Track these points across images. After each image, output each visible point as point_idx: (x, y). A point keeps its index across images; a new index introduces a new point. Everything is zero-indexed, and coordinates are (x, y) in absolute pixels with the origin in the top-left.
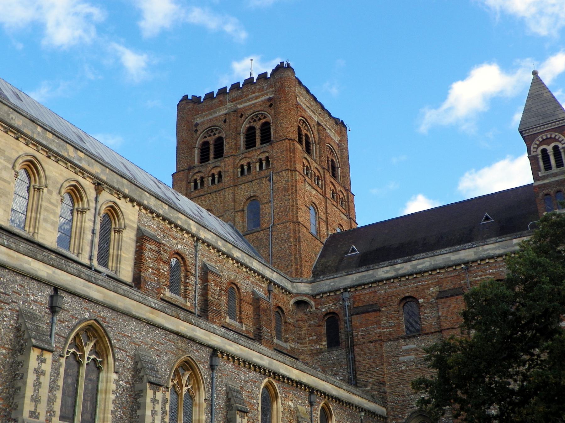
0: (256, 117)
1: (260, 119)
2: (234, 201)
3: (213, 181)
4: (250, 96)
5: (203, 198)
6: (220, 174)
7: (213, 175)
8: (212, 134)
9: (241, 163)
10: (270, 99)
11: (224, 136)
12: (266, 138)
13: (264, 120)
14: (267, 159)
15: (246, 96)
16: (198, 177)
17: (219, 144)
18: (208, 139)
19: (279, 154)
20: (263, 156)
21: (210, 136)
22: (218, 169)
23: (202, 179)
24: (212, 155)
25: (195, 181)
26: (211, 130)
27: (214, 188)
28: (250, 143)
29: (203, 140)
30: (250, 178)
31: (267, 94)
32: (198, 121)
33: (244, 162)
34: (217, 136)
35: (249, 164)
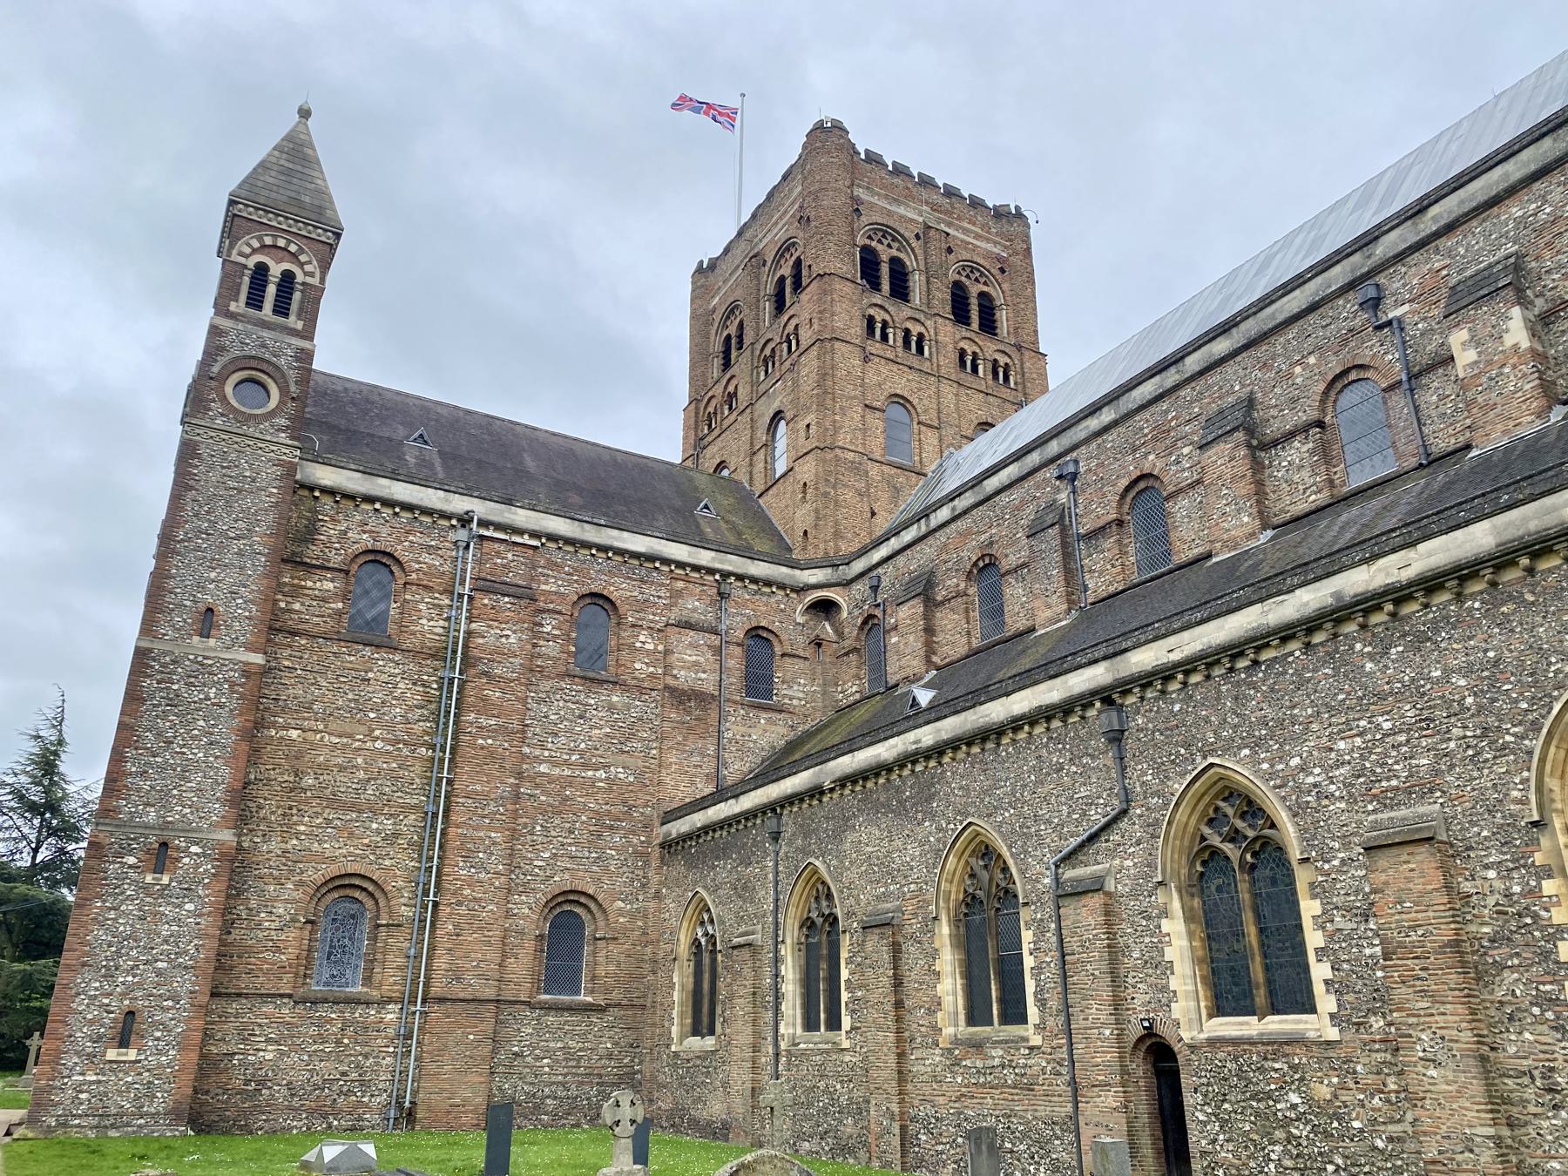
1: (977, 280)
4: (966, 225)
5: (895, 368)
6: (921, 337)
8: (886, 242)
13: (985, 289)
14: (1007, 368)
15: (959, 218)
19: (1035, 376)
21: (880, 241)
26: (885, 232)
27: (914, 361)
29: (868, 242)
31: (995, 243)
34: (894, 253)
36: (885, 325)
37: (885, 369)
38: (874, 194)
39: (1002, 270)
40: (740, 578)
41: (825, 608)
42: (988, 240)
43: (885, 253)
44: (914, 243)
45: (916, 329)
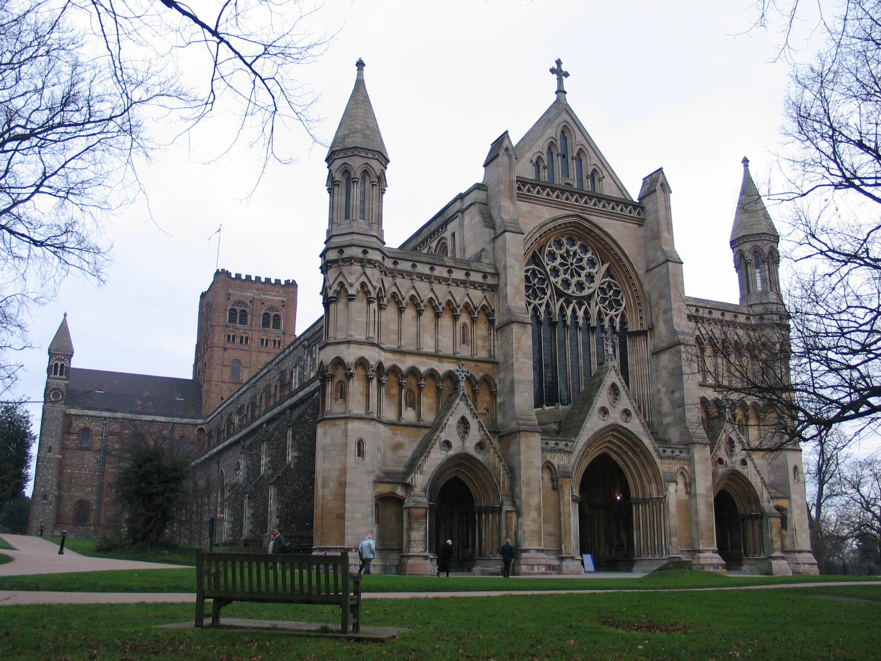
0: (272, 308)
2: (257, 361)
3: (241, 342)
4: (270, 293)
7: (242, 338)
9: (263, 337)
10: (283, 301)
11: (248, 311)
12: (277, 325)
13: (277, 313)
14: (279, 342)
16: (231, 334)
17: (244, 314)
18: (235, 307)
20: (277, 339)
22: (246, 335)
23: (234, 337)
24: (238, 321)
25: (229, 336)
26: (239, 303)
27: (243, 347)
28: (266, 324)
30: (267, 350)
31: (281, 296)
32: (230, 291)
33: (265, 338)
34: (242, 308)
35: (267, 340)
36: (234, 337)
37: (231, 352)
38: (235, 290)
39: (283, 306)
40: (178, 424)
41: (201, 430)
42: (279, 296)
43: (238, 309)
44: (249, 304)
45: (245, 336)
